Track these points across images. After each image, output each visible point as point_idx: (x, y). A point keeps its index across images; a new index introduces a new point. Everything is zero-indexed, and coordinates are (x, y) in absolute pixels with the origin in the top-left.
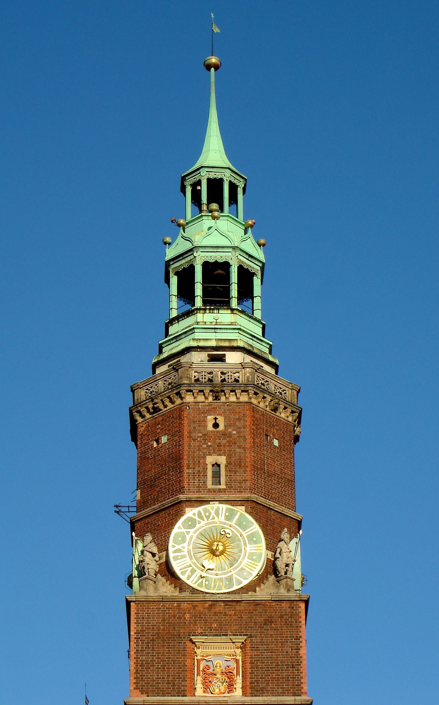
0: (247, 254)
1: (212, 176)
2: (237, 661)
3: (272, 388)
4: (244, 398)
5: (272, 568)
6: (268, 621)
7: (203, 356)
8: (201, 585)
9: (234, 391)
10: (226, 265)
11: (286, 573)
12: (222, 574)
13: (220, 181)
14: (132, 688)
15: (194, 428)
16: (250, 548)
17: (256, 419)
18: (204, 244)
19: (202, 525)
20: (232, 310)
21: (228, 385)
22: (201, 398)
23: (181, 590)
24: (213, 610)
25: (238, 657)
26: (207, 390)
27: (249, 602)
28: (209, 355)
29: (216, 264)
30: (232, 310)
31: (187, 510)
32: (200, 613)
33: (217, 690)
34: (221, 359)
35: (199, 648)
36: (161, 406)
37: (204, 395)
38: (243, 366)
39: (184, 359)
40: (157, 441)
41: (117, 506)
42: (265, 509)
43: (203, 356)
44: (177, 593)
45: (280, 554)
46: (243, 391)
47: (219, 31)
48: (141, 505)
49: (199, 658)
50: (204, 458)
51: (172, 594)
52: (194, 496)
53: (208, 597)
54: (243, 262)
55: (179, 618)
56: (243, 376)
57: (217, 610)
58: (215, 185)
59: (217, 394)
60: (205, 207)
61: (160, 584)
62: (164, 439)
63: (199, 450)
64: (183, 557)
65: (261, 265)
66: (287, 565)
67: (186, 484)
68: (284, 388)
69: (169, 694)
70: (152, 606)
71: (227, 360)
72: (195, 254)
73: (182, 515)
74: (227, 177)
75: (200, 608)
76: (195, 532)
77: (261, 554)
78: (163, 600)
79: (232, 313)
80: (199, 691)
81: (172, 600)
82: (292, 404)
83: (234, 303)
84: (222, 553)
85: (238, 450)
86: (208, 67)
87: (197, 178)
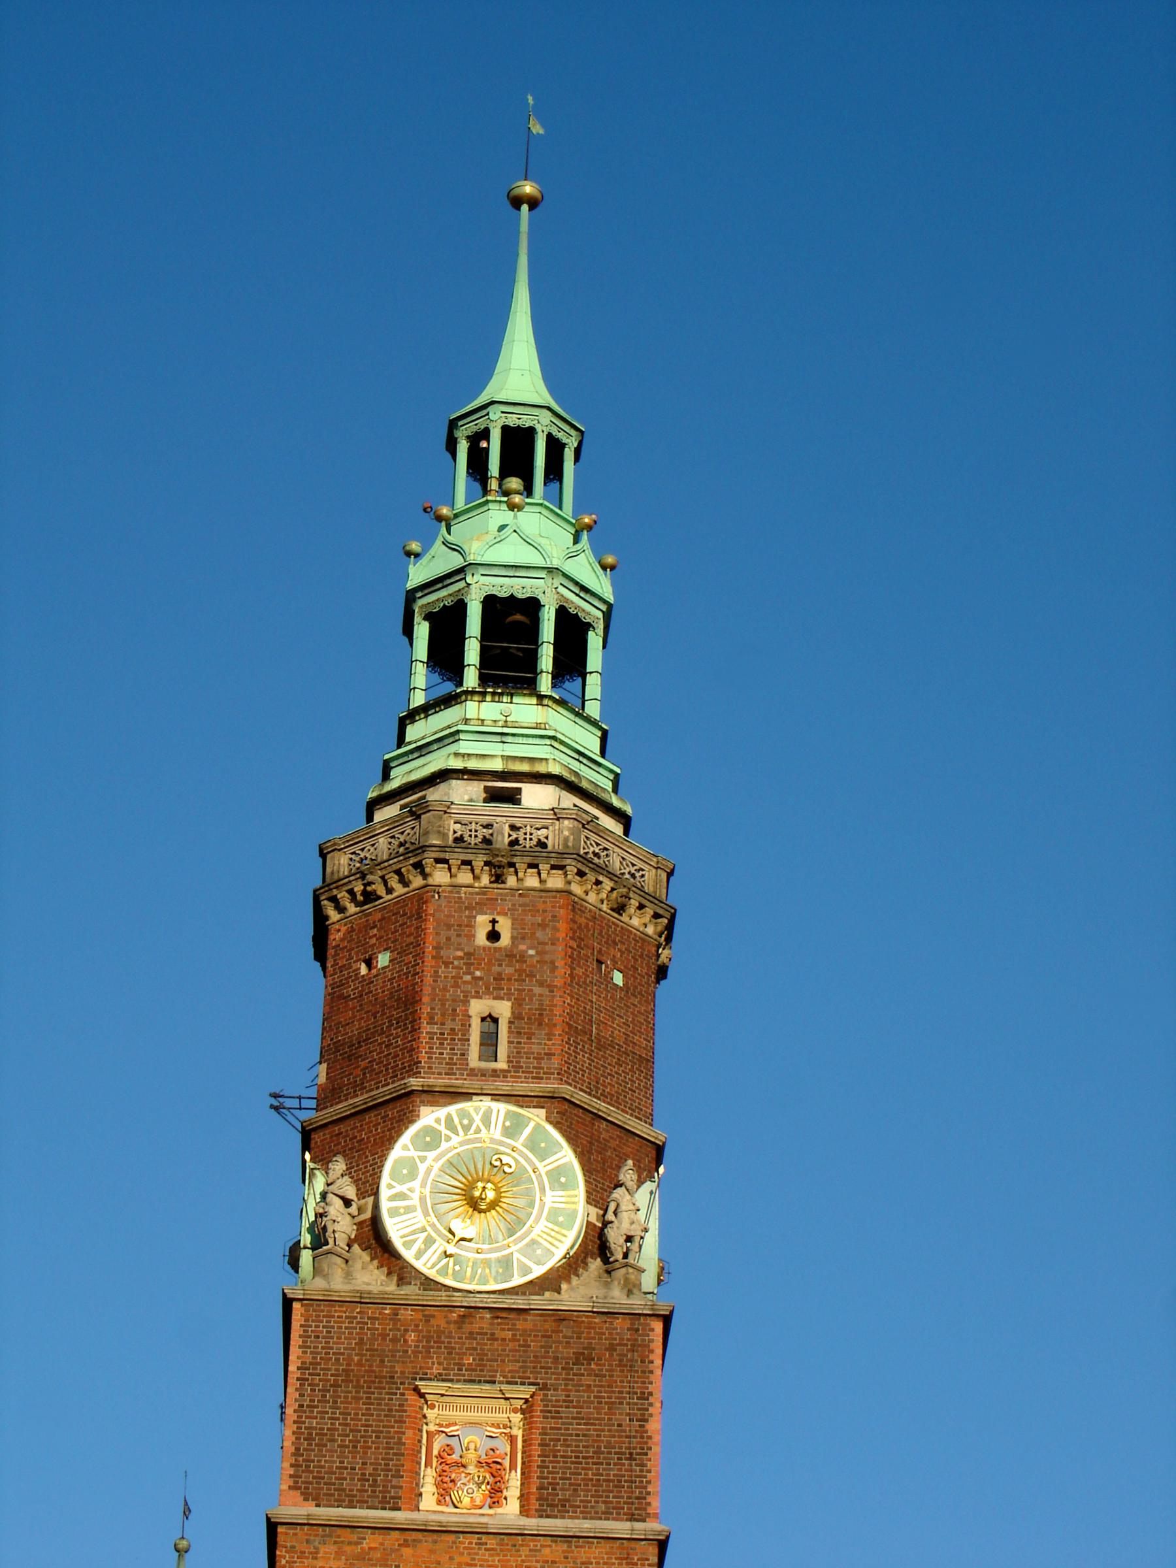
0: (577, 583)
1: (512, 421)
2: (512, 1439)
3: (615, 863)
4: (556, 881)
5: (597, 1245)
6: (584, 1357)
8: (444, 1271)
9: (536, 866)
10: (532, 606)
11: (626, 1256)
12: (491, 1251)
14: (285, 1487)
15: (448, 939)
16: (553, 1198)
17: (580, 927)
18: (489, 558)
19: (454, 1144)
20: (541, 697)
21: (524, 853)
22: (465, 877)
23: (401, 1281)
24: (467, 1328)
25: (515, 1431)
26: (479, 863)
27: (544, 1313)
28: (486, 789)
29: (512, 602)
30: (541, 697)
31: (424, 1110)
32: (439, 1333)
33: (466, 1501)
34: (512, 797)
35: (432, 1407)
36: (381, 891)
37: (473, 870)
38: (557, 815)
39: (434, 795)
40: (369, 963)
41: (275, 1096)
42: (588, 1118)
44: (392, 1287)
45: (615, 1213)
46: (553, 867)
47: (541, 132)
49: (432, 1428)
50: (466, 1002)
51: (381, 1288)
52: (439, 1082)
53: (458, 1299)
54: (567, 600)
55: (395, 1340)
56: (557, 835)
57: (476, 1327)
58: (518, 441)
59: (499, 871)
60: (494, 485)
61: (358, 1265)
62: (383, 960)
63: (456, 985)
64: (409, 1210)
65: (604, 608)
66: (629, 1239)
67: (423, 1056)
68: (640, 865)
69: (364, 1504)
70: (337, 1311)
71: (523, 801)
72: (469, 579)
73: (412, 1122)
74: (543, 424)
75: (439, 1321)
76: (436, 1160)
77: (575, 1212)
78: (362, 1300)
79: (540, 704)
80: (429, 1501)
81: (380, 1302)
82: (655, 899)
83: (545, 684)
84: (493, 1205)
85: (537, 990)
86: (517, 202)
87: (482, 424)
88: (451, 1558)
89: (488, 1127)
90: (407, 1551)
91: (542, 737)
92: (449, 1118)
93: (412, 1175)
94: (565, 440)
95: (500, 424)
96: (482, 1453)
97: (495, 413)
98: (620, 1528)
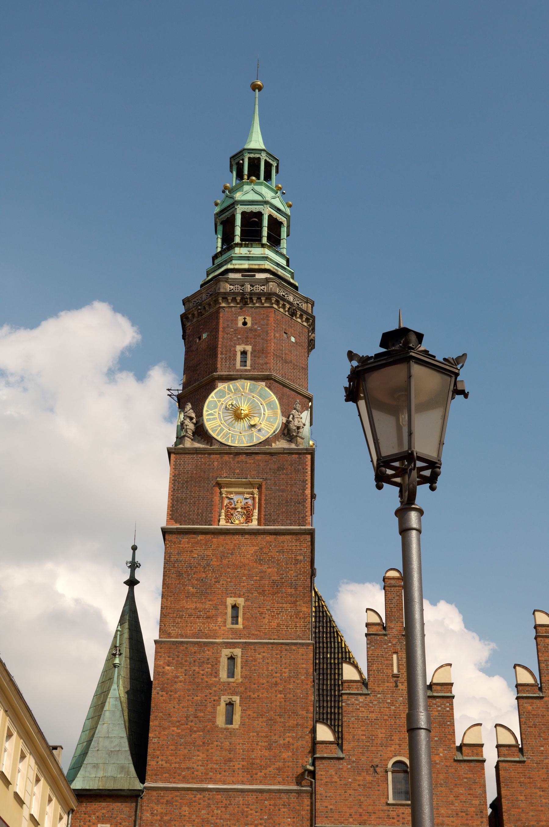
1: (252, 156)
10: (260, 215)
24: (237, 460)
33: (237, 522)
40: (200, 339)
41: (169, 390)
55: (209, 465)
60: (246, 177)
62: (204, 336)
63: (231, 341)
64: (215, 419)
66: (298, 428)
67: (219, 366)
73: (215, 389)
80: (223, 522)
83: (265, 240)
88: (231, 542)
90: (215, 540)
92: (229, 387)
93: (215, 407)
96: (243, 504)
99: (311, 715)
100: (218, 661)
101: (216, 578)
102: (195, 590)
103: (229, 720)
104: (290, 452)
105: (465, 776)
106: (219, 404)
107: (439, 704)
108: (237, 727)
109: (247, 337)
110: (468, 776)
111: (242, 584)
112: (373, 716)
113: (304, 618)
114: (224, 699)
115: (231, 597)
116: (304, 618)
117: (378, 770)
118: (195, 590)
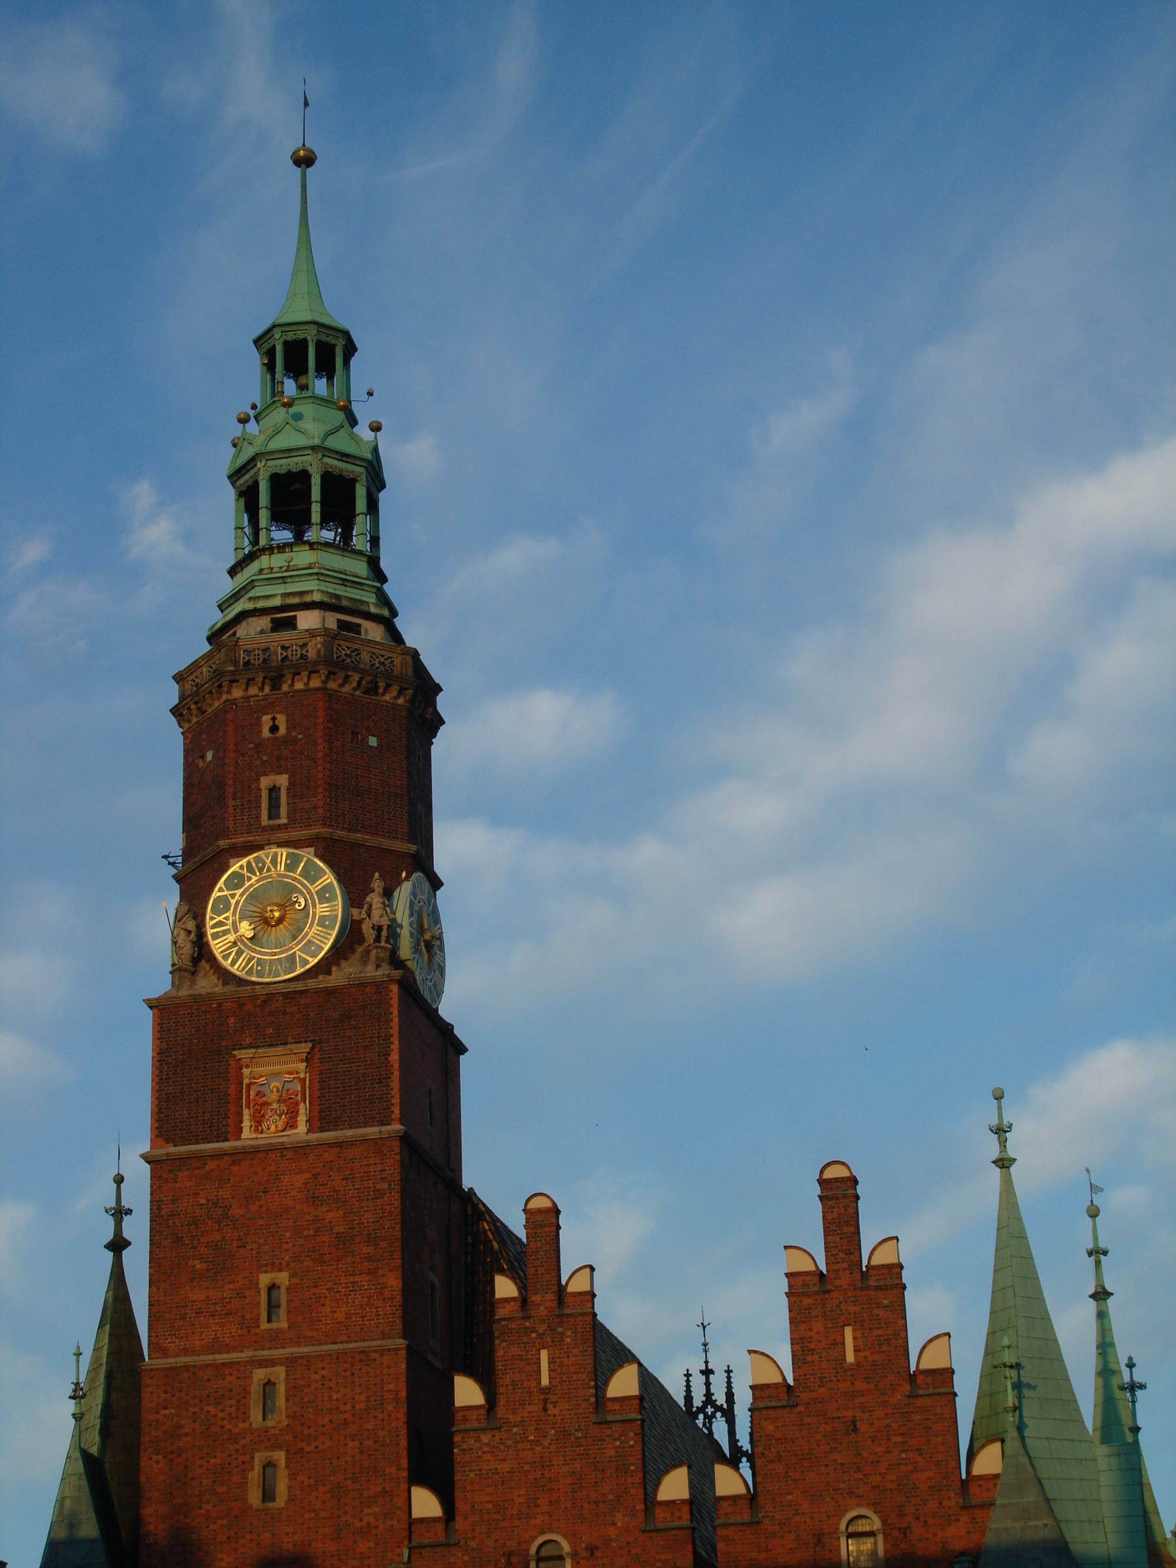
1: (290, 337)
2: (303, 1081)
7: (264, 622)
10: (304, 476)
13: (303, 343)
15: (244, 736)
16: (322, 909)
22: (253, 691)
23: (225, 983)
27: (318, 991)
28: (272, 620)
31: (232, 861)
33: (273, 1128)
34: (291, 624)
41: (166, 857)
43: (264, 622)
48: (187, 853)
50: (258, 780)
62: (209, 756)
64: (225, 932)
68: (388, 654)
76: (242, 895)
80: (246, 1133)
84: (280, 920)
89: (275, 867)
90: (235, 1168)
91: (310, 574)
93: (227, 909)
94: (333, 342)
95: (282, 340)
97: (277, 334)
98: (372, 1131)
99: (404, 1474)
100: (246, 1392)
101: (240, 1239)
102: (204, 1266)
103: (268, 1495)
104: (362, 985)
105: (658, 1557)
106: (233, 902)
107: (616, 1435)
108: (283, 1505)
109: (279, 759)
110: (663, 1557)
111: (285, 1246)
112: (505, 1467)
113: (392, 1298)
114: (259, 1458)
115: (266, 1272)
116: (392, 1298)
117: (514, 1560)
118: (204, 1266)
